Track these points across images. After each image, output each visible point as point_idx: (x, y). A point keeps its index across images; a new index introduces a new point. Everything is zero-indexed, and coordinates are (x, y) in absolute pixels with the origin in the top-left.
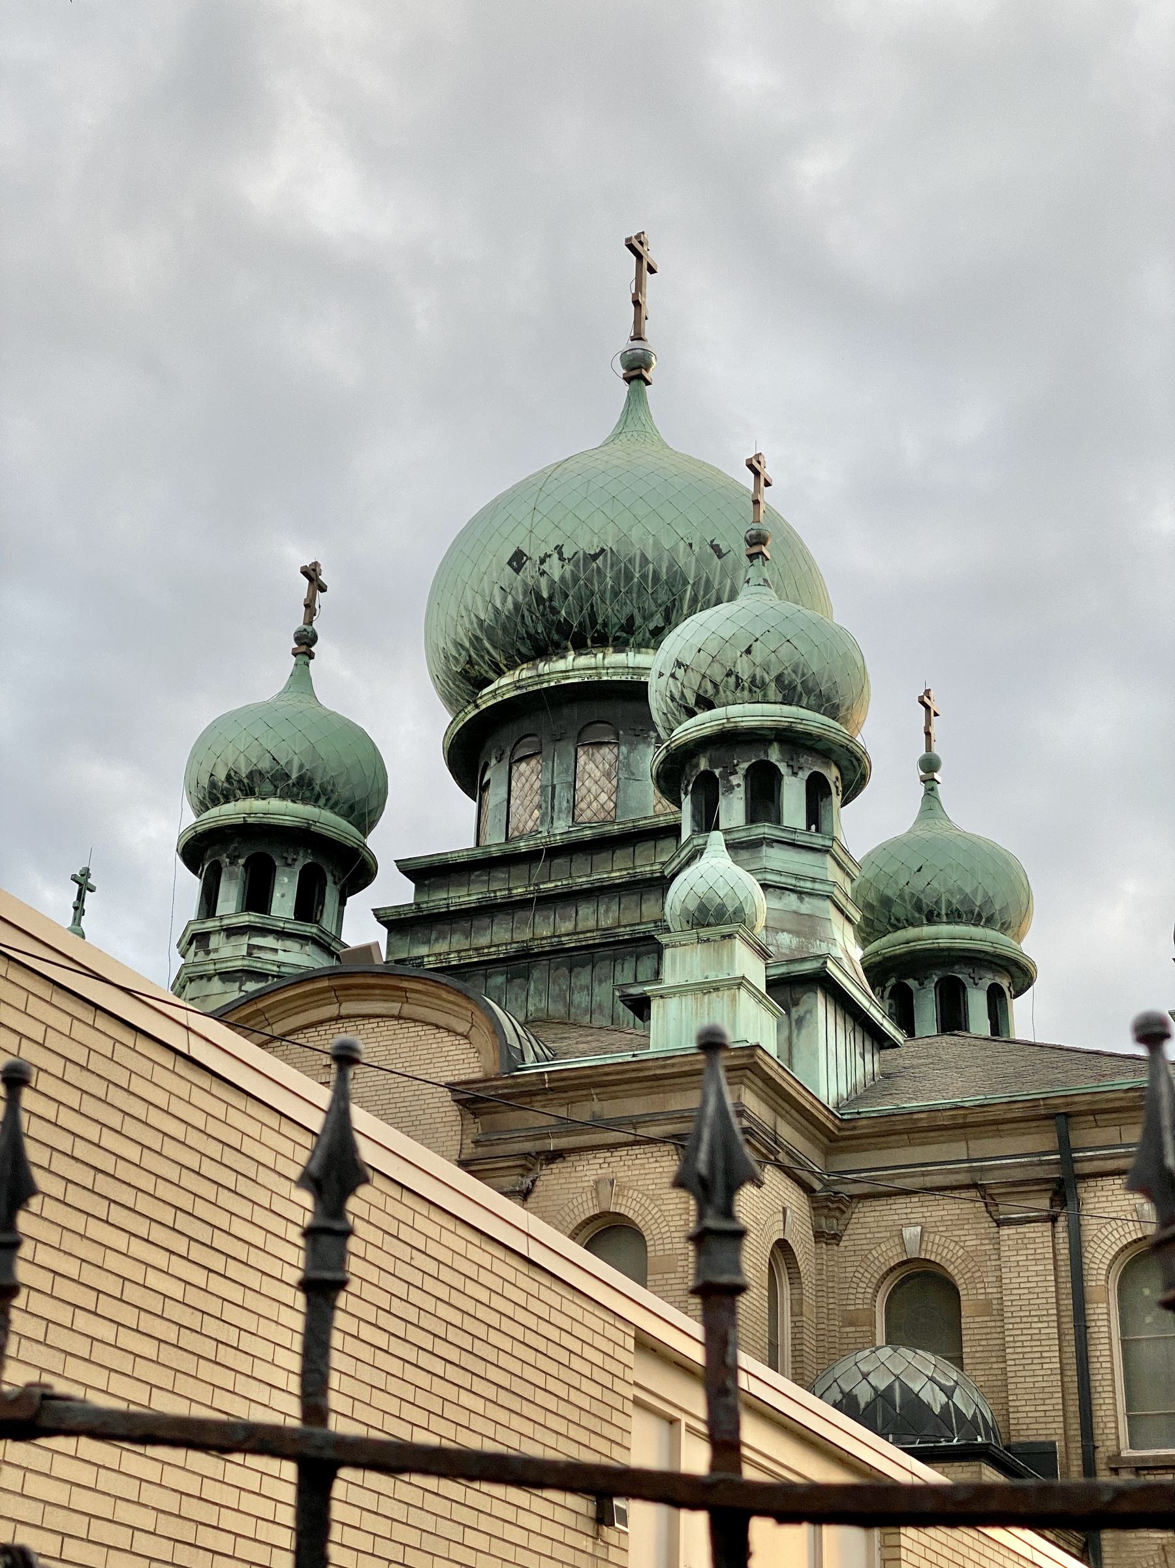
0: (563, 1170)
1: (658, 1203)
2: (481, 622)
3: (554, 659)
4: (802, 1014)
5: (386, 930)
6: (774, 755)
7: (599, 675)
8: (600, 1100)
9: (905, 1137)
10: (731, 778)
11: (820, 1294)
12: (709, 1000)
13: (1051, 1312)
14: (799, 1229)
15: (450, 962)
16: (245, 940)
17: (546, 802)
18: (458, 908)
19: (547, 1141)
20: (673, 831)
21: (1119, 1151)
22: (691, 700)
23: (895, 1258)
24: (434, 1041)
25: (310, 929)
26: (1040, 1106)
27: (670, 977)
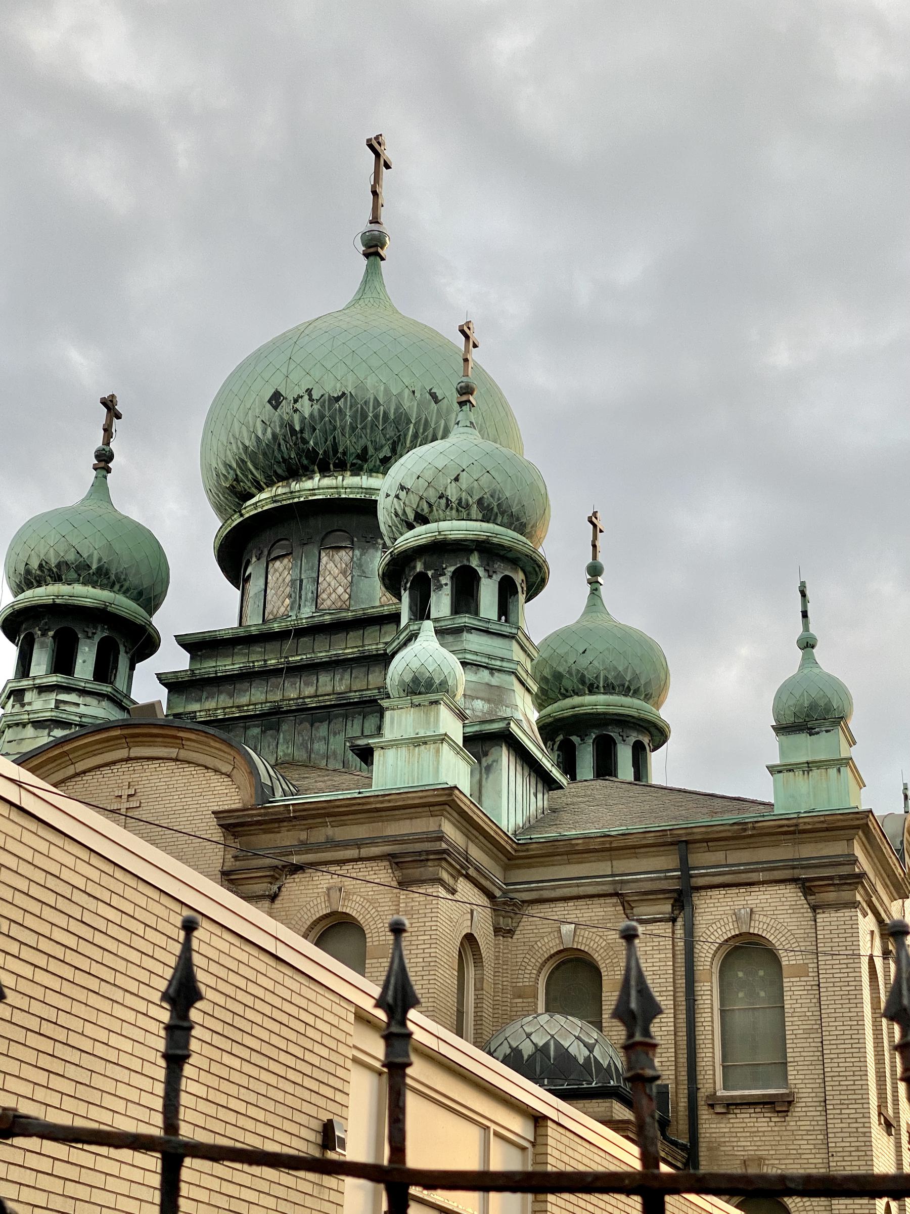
0: (303, 880)
1: (376, 905)
2: (246, 448)
3: (304, 479)
4: (490, 763)
5: (167, 690)
6: (475, 562)
7: (339, 493)
8: (332, 827)
9: (565, 857)
10: (441, 578)
11: (497, 974)
12: (419, 751)
13: (669, 988)
14: (483, 925)
15: (217, 716)
16: (53, 697)
17: (296, 593)
18: (224, 674)
19: (292, 857)
20: (395, 618)
21: (725, 869)
22: (411, 516)
23: (555, 947)
24: (204, 779)
25: (106, 689)
26: (667, 835)
27: (389, 733)
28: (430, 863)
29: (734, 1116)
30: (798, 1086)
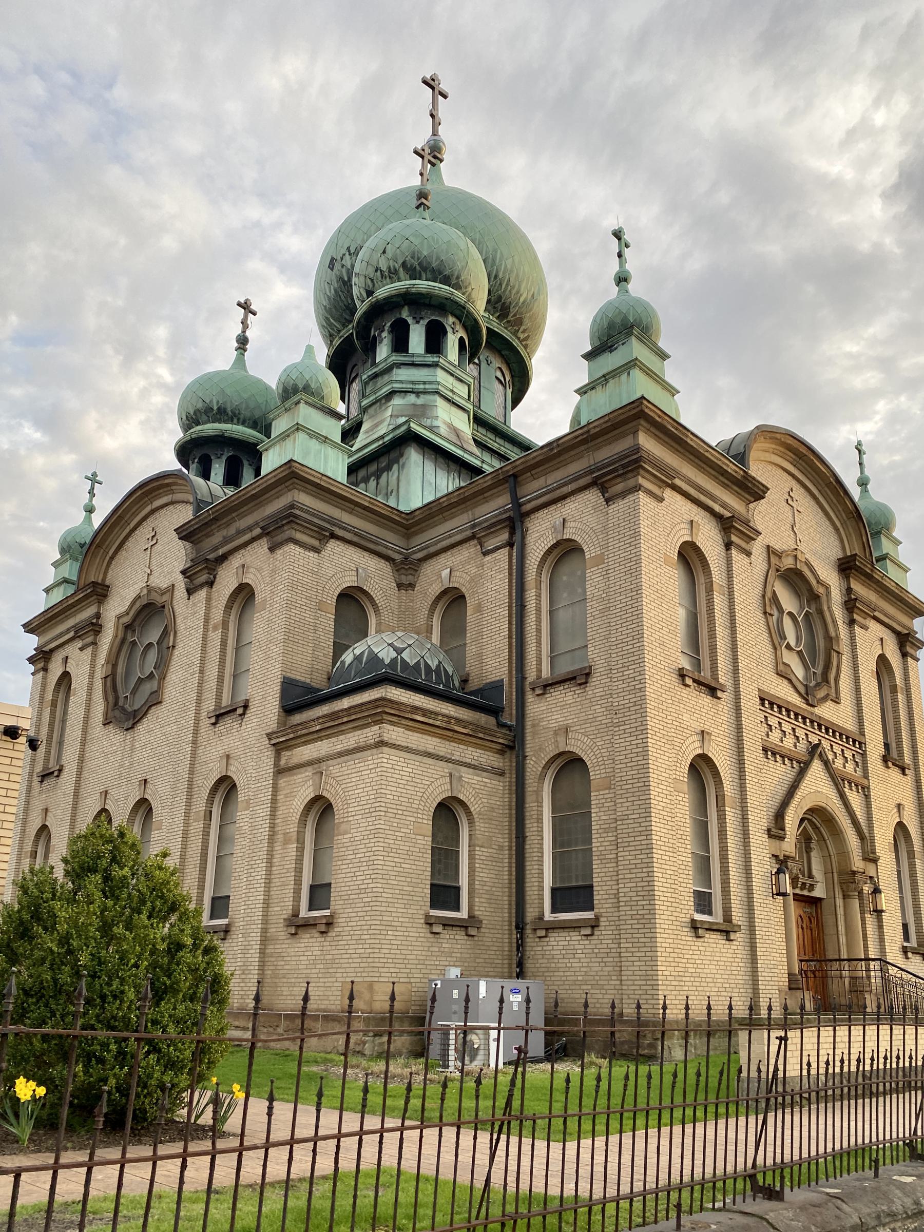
28: (285, 528)
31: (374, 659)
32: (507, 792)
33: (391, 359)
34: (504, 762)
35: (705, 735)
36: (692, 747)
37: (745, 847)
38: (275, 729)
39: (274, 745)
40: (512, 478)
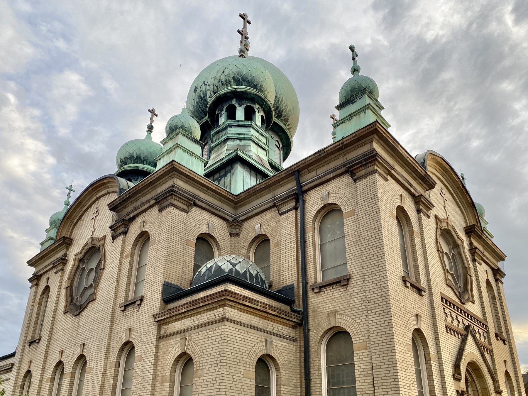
9: (255, 196)
29: (323, 293)
30: (352, 271)
31: (219, 269)
32: (298, 351)
33: (226, 123)
34: (296, 334)
35: (418, 316)
36: (412, 324)
37: (442, 385)
38: (158, 312)
39: (157, 322)
40: (297, 173)
